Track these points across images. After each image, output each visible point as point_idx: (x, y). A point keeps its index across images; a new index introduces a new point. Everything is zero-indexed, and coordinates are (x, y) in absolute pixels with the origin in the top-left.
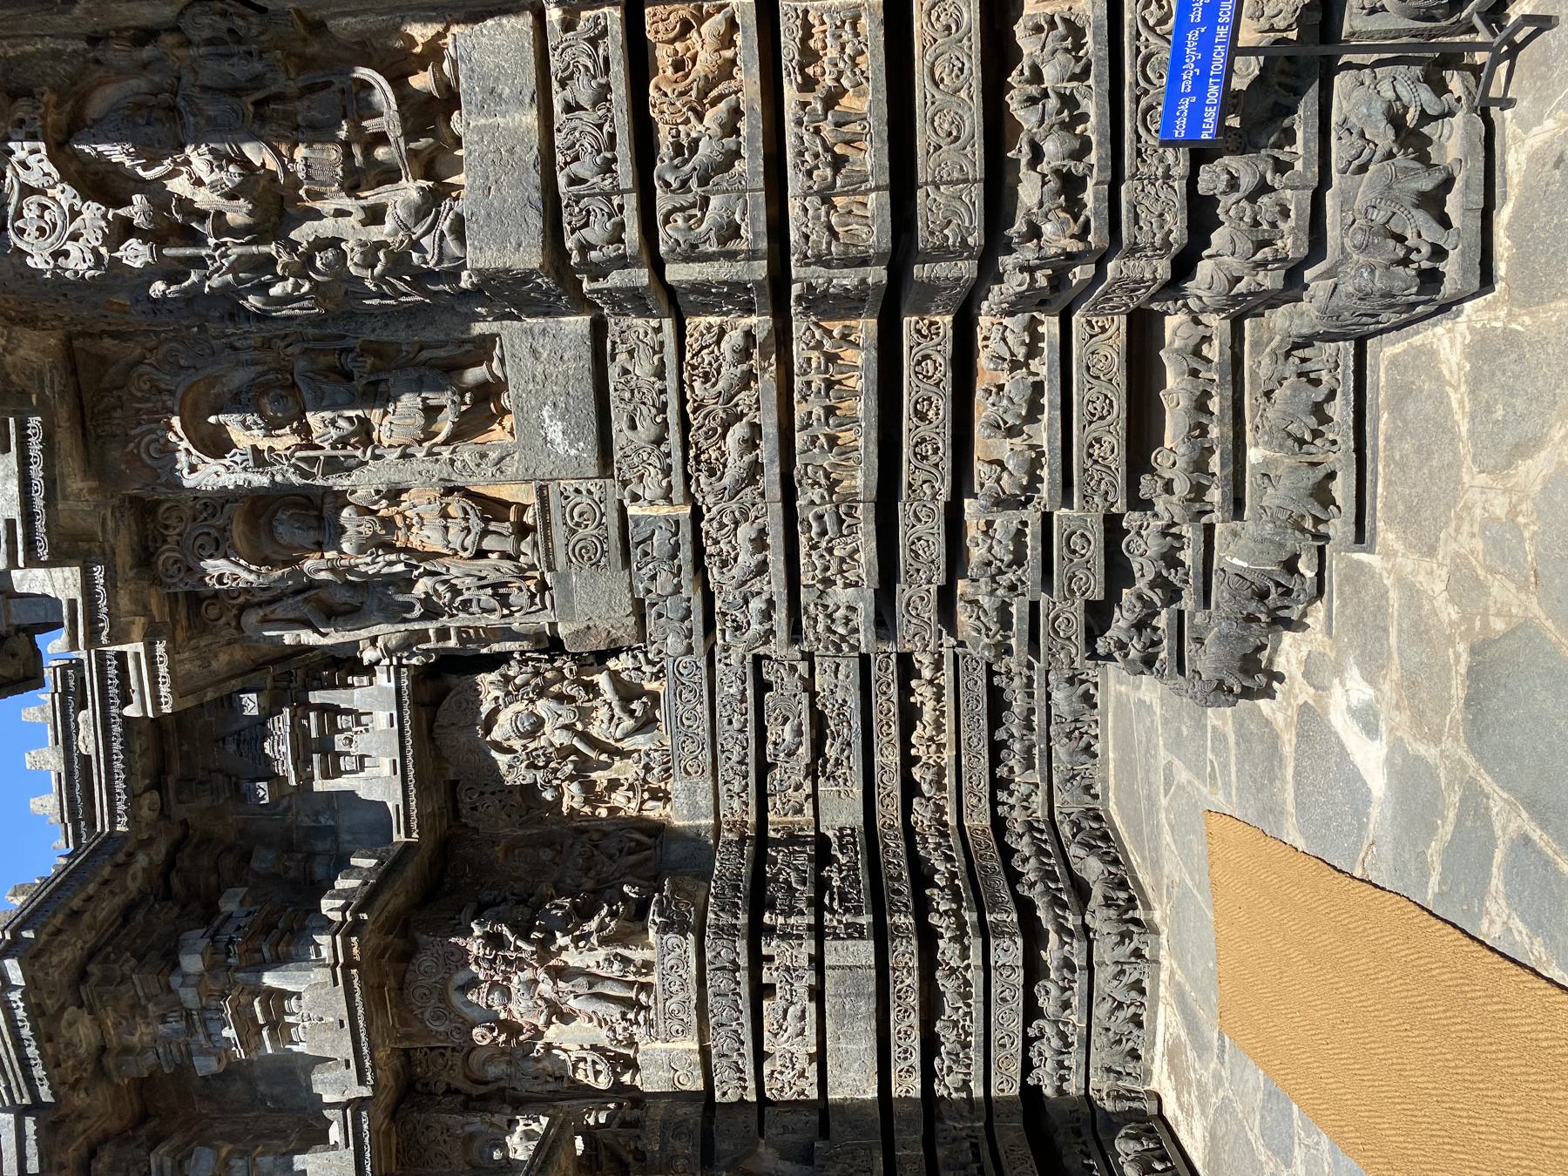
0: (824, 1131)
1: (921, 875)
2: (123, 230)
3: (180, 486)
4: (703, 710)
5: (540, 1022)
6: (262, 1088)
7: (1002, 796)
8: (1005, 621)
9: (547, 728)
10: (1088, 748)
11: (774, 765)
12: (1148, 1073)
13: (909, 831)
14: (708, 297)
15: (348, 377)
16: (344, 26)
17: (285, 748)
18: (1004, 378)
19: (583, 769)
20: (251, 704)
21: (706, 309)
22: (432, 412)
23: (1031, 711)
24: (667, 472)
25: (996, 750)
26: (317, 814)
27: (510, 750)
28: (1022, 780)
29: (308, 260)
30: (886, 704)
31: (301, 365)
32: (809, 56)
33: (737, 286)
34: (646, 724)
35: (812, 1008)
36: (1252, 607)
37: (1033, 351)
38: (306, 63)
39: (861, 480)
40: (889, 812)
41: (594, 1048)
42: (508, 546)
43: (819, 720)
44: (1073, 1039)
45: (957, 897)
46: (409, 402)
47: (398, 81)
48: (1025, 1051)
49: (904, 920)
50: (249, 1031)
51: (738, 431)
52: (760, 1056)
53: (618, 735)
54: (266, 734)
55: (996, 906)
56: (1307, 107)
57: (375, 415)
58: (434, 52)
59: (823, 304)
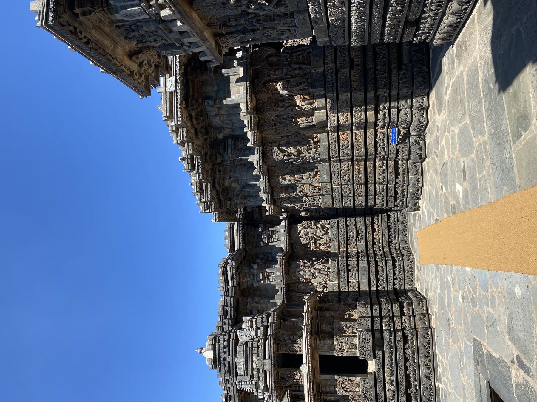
0: (360, 295)
1: (375, 255)
2: (284, 155)
3: (280, 184)
4: (336, 230)
5: (311, 278)
6: (262, 293)
7: (390, 244)
8: (383, 201)
9: (309, 234)
10: (405, 235)
11: (349, 240)
12: (415, 284)
13: (374, 251)
14: (344, 160)
15: (301, 171)
16: (307, 135)
17: (266, 237)
18: (380, 169)
19: (316, 240)
20: (260, 229)
21: (344, 162)
22: (310, 175)
23: (395, 229)
24: (339, 180)
25: (389, 236)
26: (269, 250)
27: (303, 238)
28: (394, 242)
29: (303, 158)
30: (369, 228)
31: (295, 170)
32: (356, 136)
33: (348, 159)
34: (326, 233)
35: (357, 273)
36: (413, 196)
37: (383, 165)
38: (303, 138)
39: (362, 181)
40: (370, 248)
41: (319, 283)
42: (318, 191)
43: (357, 232)
44: (402, 279)
45: (381, 256)
46: (308, 173)
47: (313, 140)
48: (394, 281)
49: (372, 259)
50: (264, 278)
51: (347, 176)
52: (348, 282)
53: (322, 235)
54: (262, 234)
55: (388, 257)
56: (407, 140)
57: (304, 175)
58: (316, 137)
59: (357, 161)
